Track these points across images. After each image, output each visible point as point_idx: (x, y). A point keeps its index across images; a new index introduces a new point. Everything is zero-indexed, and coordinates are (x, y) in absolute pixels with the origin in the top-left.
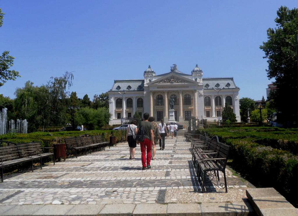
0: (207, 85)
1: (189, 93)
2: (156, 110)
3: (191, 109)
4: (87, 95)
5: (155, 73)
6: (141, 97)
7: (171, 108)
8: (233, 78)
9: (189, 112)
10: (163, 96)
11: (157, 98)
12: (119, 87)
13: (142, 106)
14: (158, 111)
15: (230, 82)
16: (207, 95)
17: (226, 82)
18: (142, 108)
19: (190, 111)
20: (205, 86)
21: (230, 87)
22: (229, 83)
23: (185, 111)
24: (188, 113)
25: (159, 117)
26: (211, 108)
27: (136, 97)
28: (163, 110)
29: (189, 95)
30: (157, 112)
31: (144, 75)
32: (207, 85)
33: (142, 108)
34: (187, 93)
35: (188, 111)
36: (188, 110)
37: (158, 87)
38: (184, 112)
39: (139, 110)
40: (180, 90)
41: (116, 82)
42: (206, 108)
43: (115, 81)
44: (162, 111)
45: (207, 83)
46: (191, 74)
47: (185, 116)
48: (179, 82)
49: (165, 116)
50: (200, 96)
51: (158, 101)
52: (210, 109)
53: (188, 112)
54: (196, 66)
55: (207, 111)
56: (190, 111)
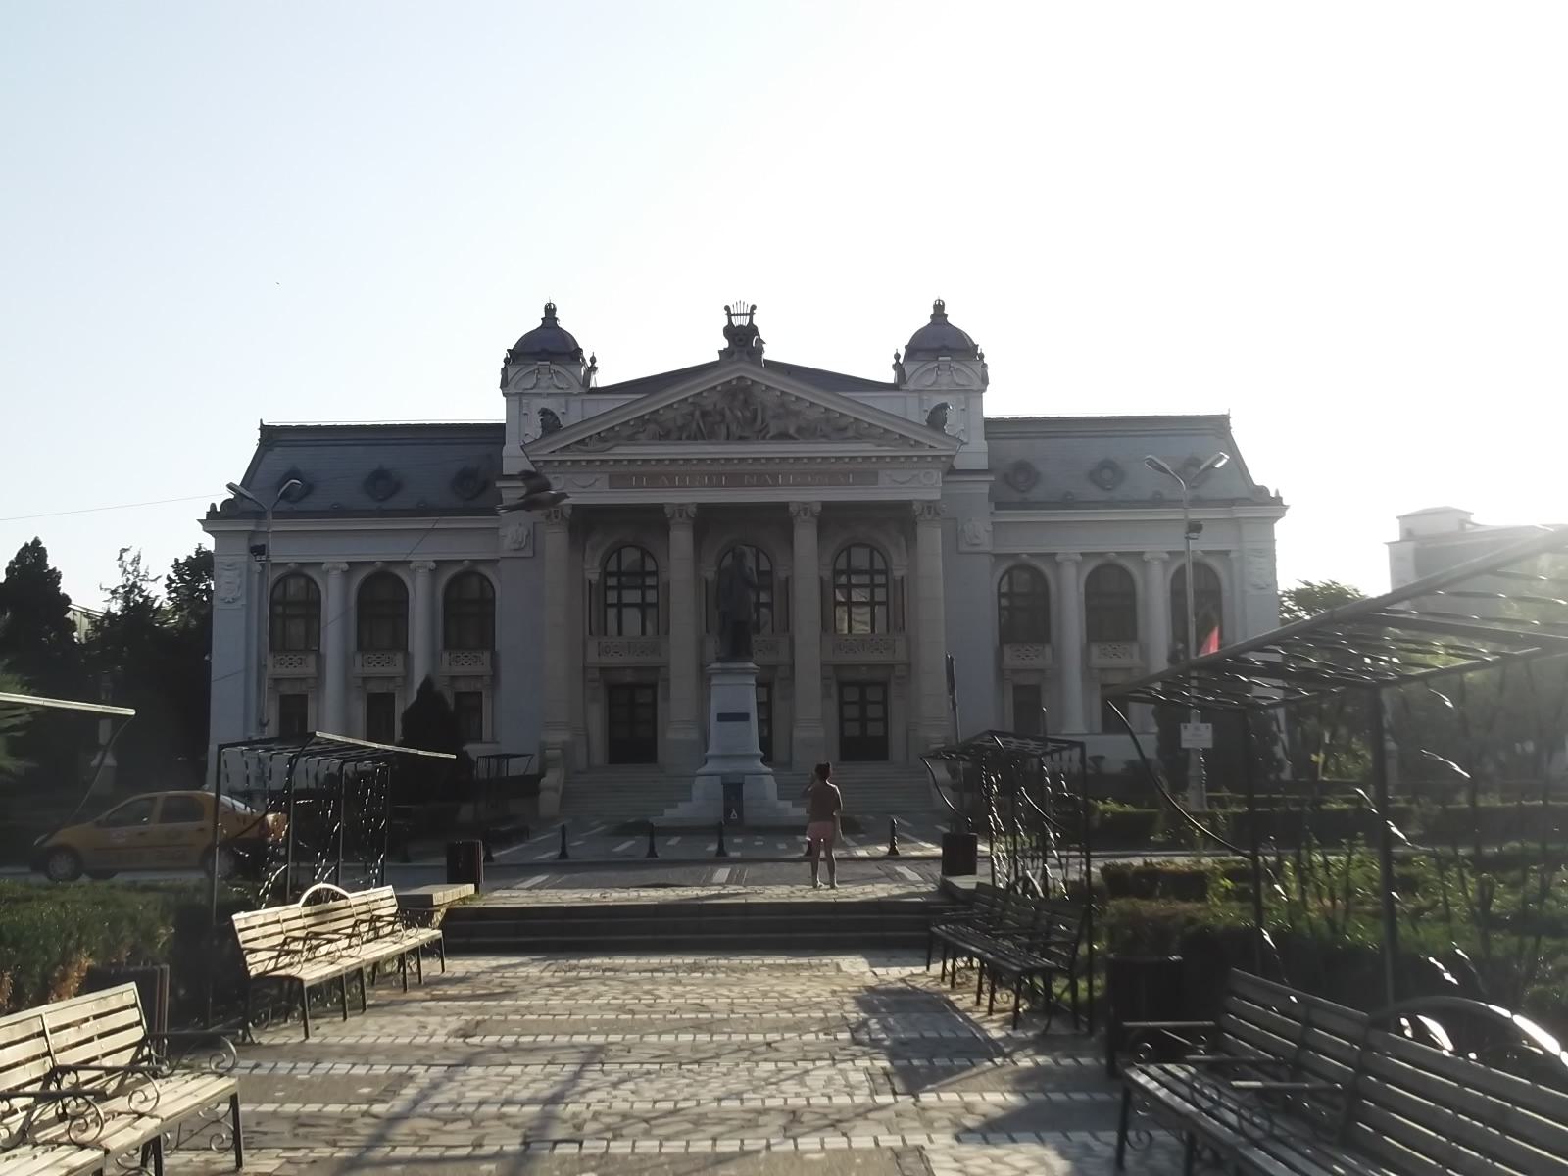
2: (603, 670)
4: (37, 542)
9: (874, 694)
13: (486, 639)
18: (486, 656)
23: (842, 685)
28: (656, 669)
33: (486, 656)
35: (863, 686)
37: (619, 479)
38: (834, 691)
39: (458, 670)
40: (805, 506)
43: (264, 429)
47: (842, 720)
48: (792, 431)
51: (612, 597)
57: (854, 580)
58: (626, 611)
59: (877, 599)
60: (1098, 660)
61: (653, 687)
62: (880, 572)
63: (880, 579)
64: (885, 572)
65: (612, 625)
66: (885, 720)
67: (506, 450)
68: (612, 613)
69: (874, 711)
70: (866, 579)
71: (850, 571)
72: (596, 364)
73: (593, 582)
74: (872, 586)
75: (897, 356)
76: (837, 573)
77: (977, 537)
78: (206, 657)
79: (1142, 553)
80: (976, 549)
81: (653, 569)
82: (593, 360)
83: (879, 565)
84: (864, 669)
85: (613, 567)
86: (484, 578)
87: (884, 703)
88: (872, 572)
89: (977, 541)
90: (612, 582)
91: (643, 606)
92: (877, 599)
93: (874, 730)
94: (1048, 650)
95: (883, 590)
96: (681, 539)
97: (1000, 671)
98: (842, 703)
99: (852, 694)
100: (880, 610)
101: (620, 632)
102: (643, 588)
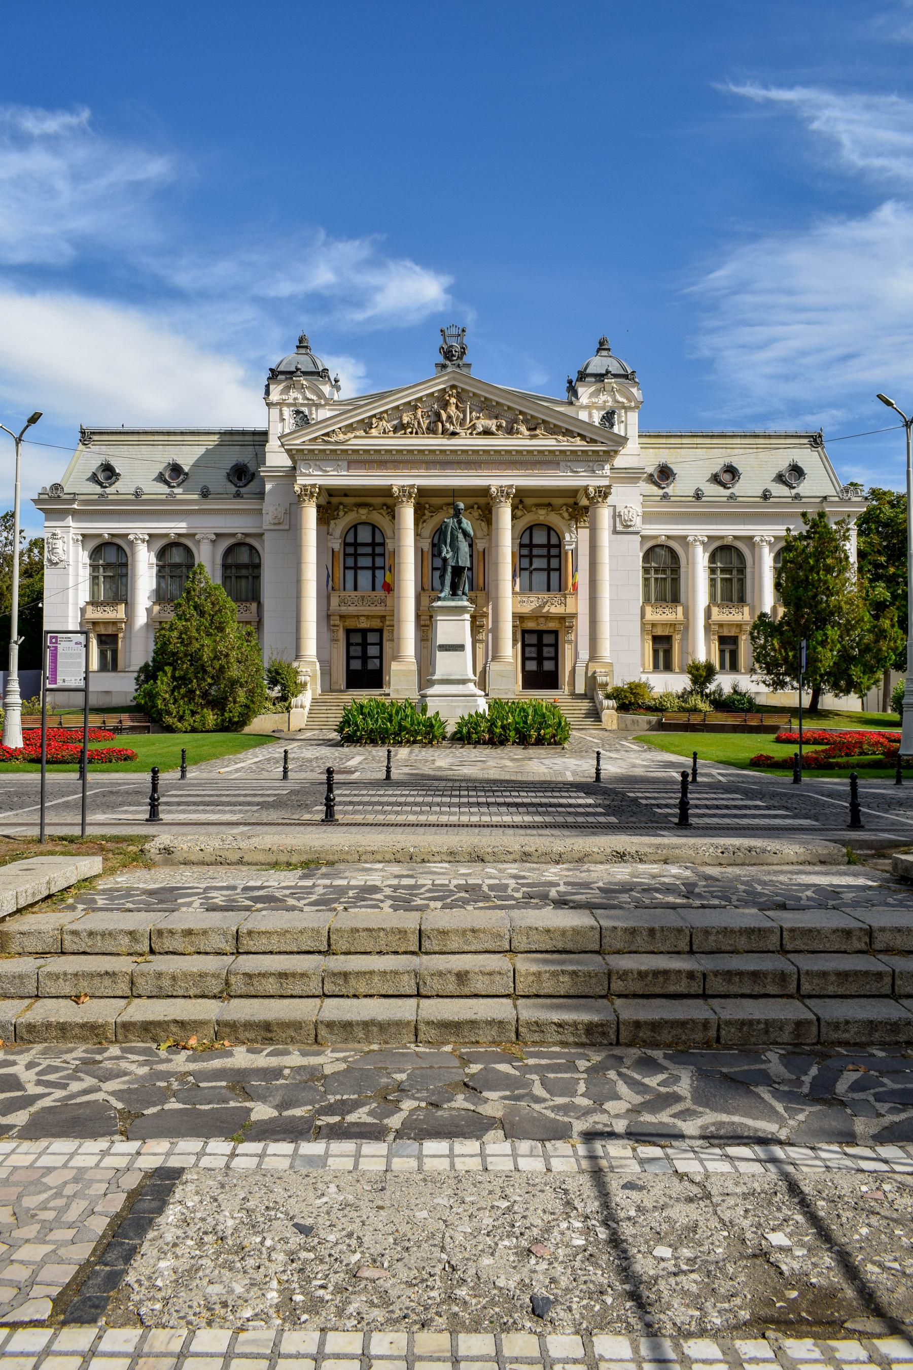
0: (665, 474)
1: (554, 519)
3: (562, 619)
5: (338, 389)
6: (246, 535)
7: (447, 590)
8: (820, 436)
9: (548, 639)
10: (389, 533)
11: (346, 544)
12: (109, 472)
14: (351, 624)
15: (808, 458)
16: (661, 530)
17: (781, 460)
18: (254, 606)
19: (556, 633)
20: (651, 479)
21: (805, 488)
22: (800, 464)
23: (524, 632)
24: (540, 646)
25: (356, 665)
26: (686, 614)
27: (217, 535)
28: (383, 617)
29: (549, 529)
30: (349, 632)
31: (267, 393)
32: (665, 474)
33: (254, 606)
34: (542, 516)
35: (540, 633)
36: (542, 627)
38: (519, 636)
41: (86, 436)
42: (652, 615)
43: (83, 433)
44: (376, 624)
45: (663, 461)
46: (564, 396)
49: (396, 657)
50: (622, 527)
51: (350, 562)
52: (673, 625)
53: (540, 639)
54: (599, 350)
55: (659, 632)
56: (556, 633)
57: (535, 551)
58: (359, 572)
59: (552, 567)
60: (717, 615)
61: (380, 631)
62: (555, 546)
63: (554, 551)
64: (559, 546)
65: (350, 584)
66: (555, 659)
67: (268, 447)
68: (350, 574)
69: (548, 652)
70: (544, 551)
71: (531, 546)
72: (339, 383)
73: (336, 550)
74: (549, 557)
75: (570, 382)
76: (521, 546)
77: (631, 521)
78: (40, 605)
79: (754, 536)
80: (631, 529)
81: (382, 541)
82: (336, 381)
83: (554, 541)
84: (542, 619)
85: (350, 539)
86: (252, 548)
87: (556, 646)
88: (549, 546)
89: (633, 523)
90: (351, 550)
91: (373, 568)
92: (552, 567)
93: (548, 666)
94: (680, 609)
95: (557, 560)
96: (408, 514)
97: (643, 624)
98: (524, 646)
99: (533, 639)
100: (554, 576)
101: (356, 589)
102: (374, 555)
